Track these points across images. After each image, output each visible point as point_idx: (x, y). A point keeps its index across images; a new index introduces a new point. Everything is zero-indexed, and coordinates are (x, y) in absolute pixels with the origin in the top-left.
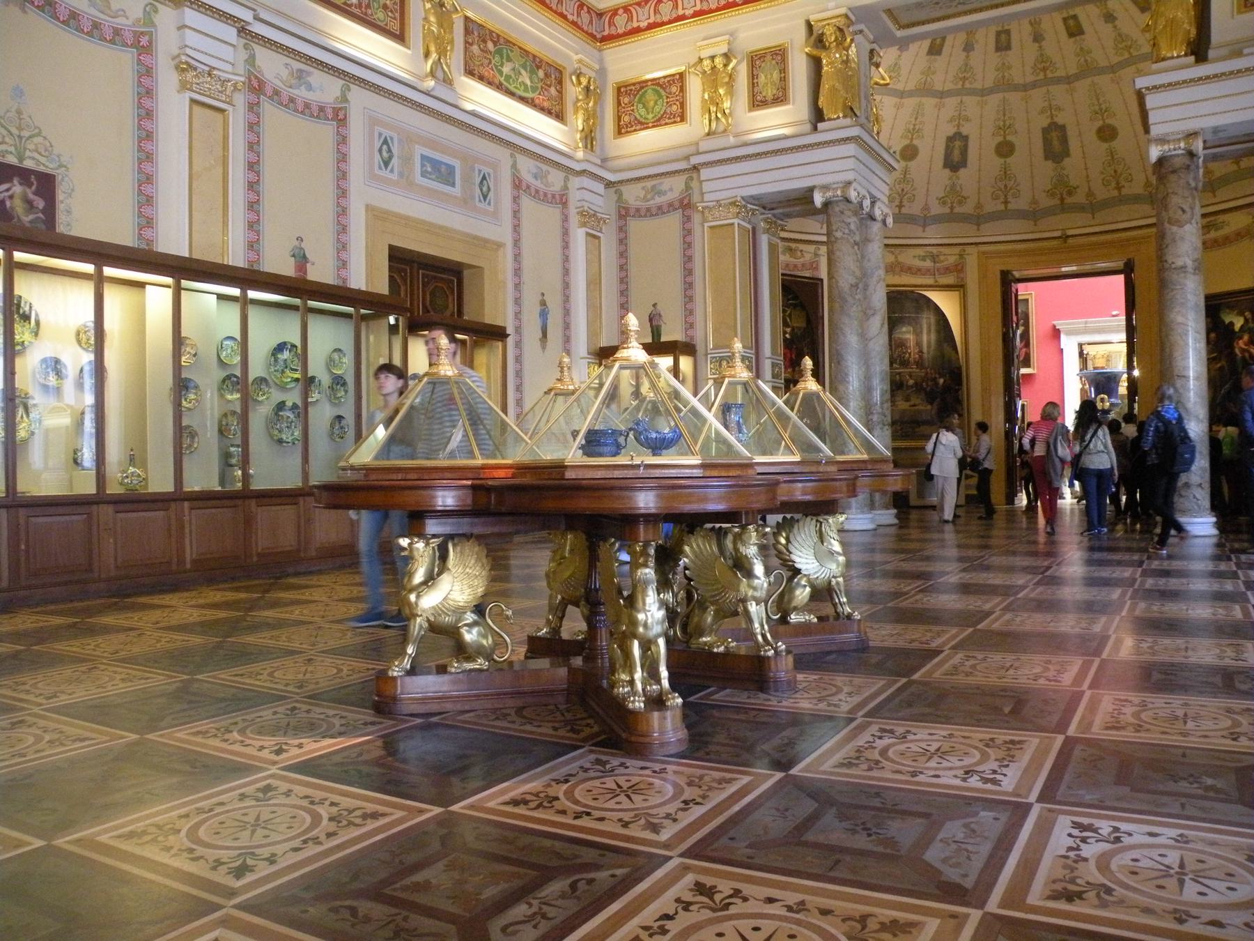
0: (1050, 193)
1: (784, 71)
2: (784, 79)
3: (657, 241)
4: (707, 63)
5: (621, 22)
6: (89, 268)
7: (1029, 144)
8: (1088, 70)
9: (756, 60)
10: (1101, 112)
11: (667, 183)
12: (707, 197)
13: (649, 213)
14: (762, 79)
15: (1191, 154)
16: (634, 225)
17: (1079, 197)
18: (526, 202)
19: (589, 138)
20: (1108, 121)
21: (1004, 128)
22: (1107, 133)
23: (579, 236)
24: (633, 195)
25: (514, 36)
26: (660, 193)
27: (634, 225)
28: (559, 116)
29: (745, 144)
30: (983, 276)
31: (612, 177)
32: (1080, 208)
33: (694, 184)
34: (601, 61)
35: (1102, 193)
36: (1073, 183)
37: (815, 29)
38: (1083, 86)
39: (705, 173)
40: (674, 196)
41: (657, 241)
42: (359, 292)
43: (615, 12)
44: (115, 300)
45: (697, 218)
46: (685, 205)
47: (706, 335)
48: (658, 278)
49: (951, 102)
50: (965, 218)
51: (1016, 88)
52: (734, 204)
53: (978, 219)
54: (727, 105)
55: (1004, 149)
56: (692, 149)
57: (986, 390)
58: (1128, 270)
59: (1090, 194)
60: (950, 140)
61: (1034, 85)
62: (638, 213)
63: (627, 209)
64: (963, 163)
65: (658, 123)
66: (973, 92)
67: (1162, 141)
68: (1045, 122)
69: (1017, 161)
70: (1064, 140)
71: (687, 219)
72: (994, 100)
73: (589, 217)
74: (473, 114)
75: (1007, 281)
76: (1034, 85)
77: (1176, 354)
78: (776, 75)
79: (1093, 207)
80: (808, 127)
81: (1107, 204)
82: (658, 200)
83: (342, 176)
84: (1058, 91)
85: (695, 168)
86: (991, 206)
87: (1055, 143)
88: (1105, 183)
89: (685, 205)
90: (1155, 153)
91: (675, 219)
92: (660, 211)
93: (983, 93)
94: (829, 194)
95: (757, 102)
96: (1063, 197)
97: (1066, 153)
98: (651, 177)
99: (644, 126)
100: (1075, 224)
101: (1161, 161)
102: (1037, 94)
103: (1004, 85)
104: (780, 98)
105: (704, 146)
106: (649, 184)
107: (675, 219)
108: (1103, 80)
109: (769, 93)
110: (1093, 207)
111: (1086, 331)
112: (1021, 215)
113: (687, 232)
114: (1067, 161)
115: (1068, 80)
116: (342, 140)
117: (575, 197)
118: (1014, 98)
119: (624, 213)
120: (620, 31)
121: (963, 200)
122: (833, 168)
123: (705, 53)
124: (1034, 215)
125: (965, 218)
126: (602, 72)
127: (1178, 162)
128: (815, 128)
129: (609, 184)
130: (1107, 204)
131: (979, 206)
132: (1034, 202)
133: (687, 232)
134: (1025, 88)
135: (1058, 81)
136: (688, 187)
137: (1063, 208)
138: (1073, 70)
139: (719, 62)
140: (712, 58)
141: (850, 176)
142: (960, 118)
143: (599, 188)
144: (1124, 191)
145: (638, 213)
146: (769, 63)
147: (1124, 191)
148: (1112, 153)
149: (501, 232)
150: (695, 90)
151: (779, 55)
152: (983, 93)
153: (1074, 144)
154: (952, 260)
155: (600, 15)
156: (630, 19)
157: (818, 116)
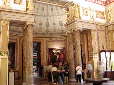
8: (42, 15)
12: (2, 18)
20: (42, 23)
22: (41, 24)
35: (38, 32)
38: (40, 17)
52: (8, 20)
80: (25, 10)
94: (30, 23)
109: (18, 2)
128: (27, 11)
130: (38, 34)
138: (40, 15)
144: (40, 32)
147: (40, 32)
157: (27, 9)
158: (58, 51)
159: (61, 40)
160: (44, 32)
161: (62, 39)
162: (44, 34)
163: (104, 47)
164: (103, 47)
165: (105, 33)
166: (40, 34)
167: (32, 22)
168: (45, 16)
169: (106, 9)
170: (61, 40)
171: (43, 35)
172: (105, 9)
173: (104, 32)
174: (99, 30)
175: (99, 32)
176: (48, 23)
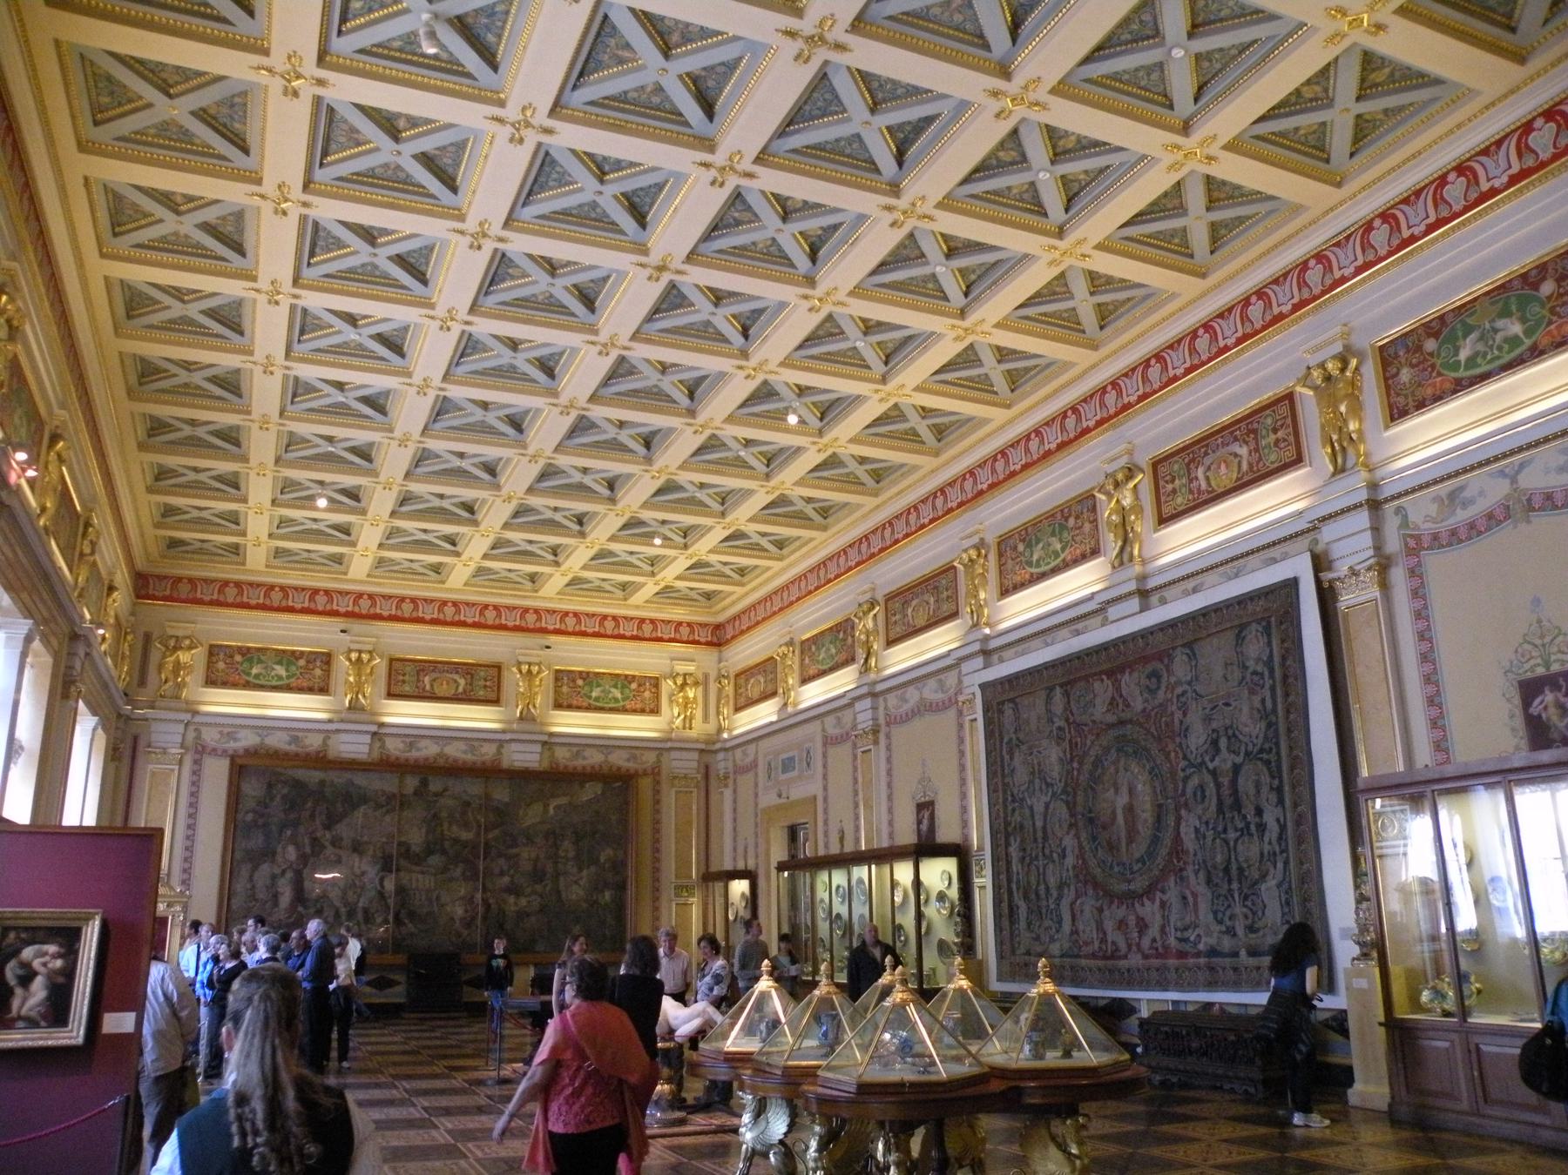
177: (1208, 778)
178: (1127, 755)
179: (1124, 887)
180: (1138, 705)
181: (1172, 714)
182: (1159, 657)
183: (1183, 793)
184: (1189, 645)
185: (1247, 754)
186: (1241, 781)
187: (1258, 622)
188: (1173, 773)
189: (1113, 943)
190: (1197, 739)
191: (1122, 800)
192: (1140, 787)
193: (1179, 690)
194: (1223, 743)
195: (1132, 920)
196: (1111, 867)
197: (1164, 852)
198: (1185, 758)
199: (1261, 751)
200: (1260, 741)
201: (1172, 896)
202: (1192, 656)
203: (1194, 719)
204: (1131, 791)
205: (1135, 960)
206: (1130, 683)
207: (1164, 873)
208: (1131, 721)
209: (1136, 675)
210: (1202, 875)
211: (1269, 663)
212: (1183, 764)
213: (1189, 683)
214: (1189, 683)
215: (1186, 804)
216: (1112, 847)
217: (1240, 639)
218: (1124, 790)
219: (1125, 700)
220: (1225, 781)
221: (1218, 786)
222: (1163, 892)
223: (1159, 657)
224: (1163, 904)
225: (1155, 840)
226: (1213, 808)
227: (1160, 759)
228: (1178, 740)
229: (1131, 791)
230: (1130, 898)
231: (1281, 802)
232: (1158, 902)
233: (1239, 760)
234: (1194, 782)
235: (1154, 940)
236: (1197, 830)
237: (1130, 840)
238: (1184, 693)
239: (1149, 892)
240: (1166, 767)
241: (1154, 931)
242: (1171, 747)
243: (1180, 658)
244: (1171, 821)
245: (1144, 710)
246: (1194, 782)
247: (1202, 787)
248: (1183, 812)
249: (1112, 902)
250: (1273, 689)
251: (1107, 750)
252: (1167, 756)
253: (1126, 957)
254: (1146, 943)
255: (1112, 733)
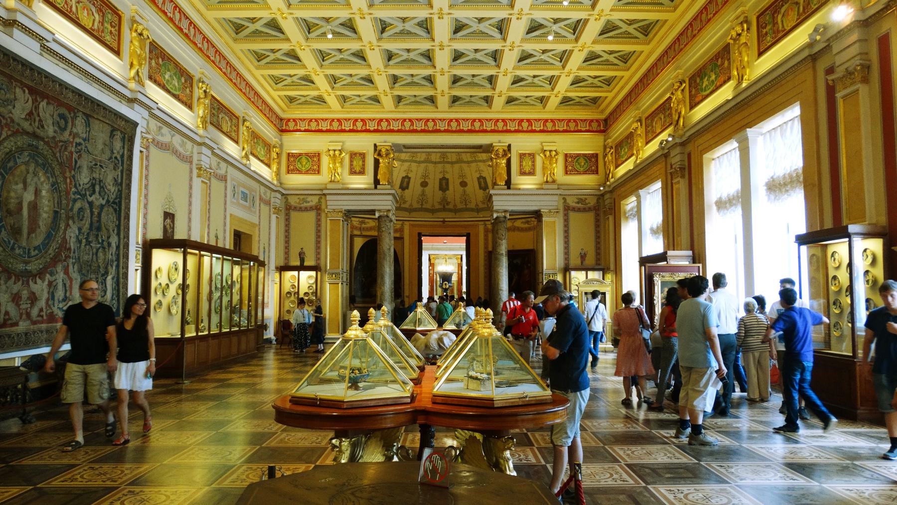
0: (440, 203)
1: (364, 161)
2: (364, 165)
3: (304, 222)
4: (331, 153)
5: (291, 125)
6: (197, 252)
7: (434, 184)
9: (353, 155)
10: (462, 176)
11: (309, 198)
13: (301, 209)
14: (355, 163)
15: (505, 217)
16: (293, 214)
17: (451, 206)
18: (262, 205)
19: (278, 174)
21: (425, 176)
22: (464, 184)
23: (274, 217)
24: (293, 201)
25: (262, 135)
26: (306, 202)
27: (293, 214)
28: (269, 166)
29: (348, 189)
30: (411, 235)
31: (284, 192)
32: (450, 210)
33: (323, 201)
34: (281, 140)
35: (460, 206)
36: (449, 200)
37: (378, 148)
38: (457, 166)
39: (328, 197)
40: (315, 204)
41: (304, 222)
42: (196, 242)
43: (289, 120)
44: (191, 261)
45: (323, 215)
46: (318, 209)
47: (327, 262)
48: (304, 238)
49: (407, 164)
50: (405, 210)
51: (432, 162)
53: (410, 210)
54: (339, 170)
55: (424, 184)
56: (323, 186)
57: (410, 283)
58: (468, 236)
59: (455, 205)
60: (403, 178)
61: (439, 163)
62: (295, 209)
63: (290, 207)
64: (407, 188)
65: (307, 172)
66: (415, 162)
67: (497, 211)
68: (441, 176)
69: (428, 190)
70: (447, 184)
71: (319, 215)
72: (423, 165)
73: (277, 210)
74: (254, 172)
75: (420, 235)
76: (439, 163)
77: (498, 284)
78: (361, 163)
79: (456, 211)
80: (373, 186)
81: (461, 210)
82: (305, 205)
83: (225, 204)
84: (448, 166)
85: (324, 195)
86: (415, 205)
87: (444, 185)
88: (461, 202)
89: (318, 209)
90: (495, 215)
91: (312, 215)
92: (306, 209)
93: (419, 162)
95: (353, 172)
96: (445, 206)
97: (448, 189)
98: (304, 193)
99: (300, 172)
100: (449, 217)
101: (497, 217)
102: (440, 166)
103: (427, 161)
104: (362, 172)
105: (329, 186)
106: (302, 197)
107: (312, 215)
108: (465, 166)
109: (358, 169)
110: (456, 211)
111: (432, 249)
112: (427, 210)
113: (318, 220)
114: (447, 192)
115: (452, 163)
116: (226, 189)
117: (273, 200)
118: (431, 167)
119: (289, 208)
120: (291, 129)
121: (405, 202)
122: (384, 203)
123: (331, 148)
124: (433, 211)
125: (405, 210)
126: (281, 146)
127: (502, 219)
128: (376, 188)
129: (283, 195)
130: (461, 210)
131: (411, 205)
132: (433, 206)
133: (318, 220)
134: (435, 163)
135: (448, 163)
136: (319, 201)
137: (444, 209)
138: (454, 160)
139: (337, 153)
140: (335, 151)
141: (390, 208)
142: (409, 170)
143: (279, 196)
145: (295, 209)
146: (358, 157)
148: (465, 191)
149: (255, 220)
150: (325, 161)
151: (363, 156)
152: (419, 162)
153: (451, 187)
154: (398, 226)
155: (281, 120)
156: (296, 125)
157: (377, 182)
158: (515, 262)
159: (526, 226)
160: (477, 205)
161: (528, 222)
162: (478, 210)
163: (585, 254)
164: (583, 257)
165: (597, 216)
166: (467, 210)
167: (389, 210)
168: (468, 162)
169: (605, 141)
170: (526, 226)
171: (475, 214)
172: (602, 144)
173: (591, 216)
174: (574, 209)
175: (572, 215)
176: (484, 178)
177: (87, 206)
178: (37, 162)
179: (21, 267)
180: (50, 131)
181: (71, 153)
182: (70, 109)
183: (72, 210)
184: (88, 116)
185: (108, 201)
186: (103, 214)
187: (121, 132)
188: (68, 193)
189: (7, 313)
190: (84, 178)
191: (29, 197)
192: (44, 193)
193: (78, 140)
194: (97, 188)
195: (25, 294)
196: (13, 249)
197: (54, 245)
198: (75, 186)
199: (114, 203)
200: (113, 197)
201: (61, 276)
202: (88, 125)
203: (84, 163)
204: (37, 192)
205: (23, 326)
206: (46, 110)
207: (55, 260)
208: (42, 139)
209: (51, 107)
210: (76, 266)
211: (122, 156)
212: (73, 189)
213: (84, 140)
214: (84, 140)
215: (73, 218)
216: (16, 232)
217: (112, 136)
218: (31, 189)
219: (40, 120)
220: (96, 211)
221: (92, 213)
222: (51, 274)
223: (70, 109)
224: (50, 284)
225: (49, 237)
226: (87, 225)
227: (60, 179)
228: (73, 172)
229: (37, 192)
230: (27, 276)
231: (118, 234)
232: (46, 283)
233: (104, 202)
234: (78, 205)
235: (41, 310)
236: (77, 237)
237: (32, 230)
238: (80, 144)
239: (41, 274)
240: (63, 186)
241: (42, 303)
242: (68, 174)
243: (80, 121)
244: (63, 226)
245: (54, 137)
246: (78, 205)
247: (81, 209)
248: (71, 222)
249: (10, 278)
250: (122, 172)
251: (21, 150)
252: (65, 178)
253: (16, 324)
254: (35, 312)
255: (26, 139)
